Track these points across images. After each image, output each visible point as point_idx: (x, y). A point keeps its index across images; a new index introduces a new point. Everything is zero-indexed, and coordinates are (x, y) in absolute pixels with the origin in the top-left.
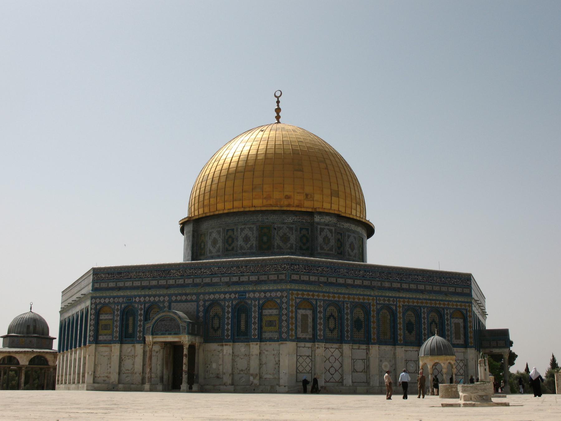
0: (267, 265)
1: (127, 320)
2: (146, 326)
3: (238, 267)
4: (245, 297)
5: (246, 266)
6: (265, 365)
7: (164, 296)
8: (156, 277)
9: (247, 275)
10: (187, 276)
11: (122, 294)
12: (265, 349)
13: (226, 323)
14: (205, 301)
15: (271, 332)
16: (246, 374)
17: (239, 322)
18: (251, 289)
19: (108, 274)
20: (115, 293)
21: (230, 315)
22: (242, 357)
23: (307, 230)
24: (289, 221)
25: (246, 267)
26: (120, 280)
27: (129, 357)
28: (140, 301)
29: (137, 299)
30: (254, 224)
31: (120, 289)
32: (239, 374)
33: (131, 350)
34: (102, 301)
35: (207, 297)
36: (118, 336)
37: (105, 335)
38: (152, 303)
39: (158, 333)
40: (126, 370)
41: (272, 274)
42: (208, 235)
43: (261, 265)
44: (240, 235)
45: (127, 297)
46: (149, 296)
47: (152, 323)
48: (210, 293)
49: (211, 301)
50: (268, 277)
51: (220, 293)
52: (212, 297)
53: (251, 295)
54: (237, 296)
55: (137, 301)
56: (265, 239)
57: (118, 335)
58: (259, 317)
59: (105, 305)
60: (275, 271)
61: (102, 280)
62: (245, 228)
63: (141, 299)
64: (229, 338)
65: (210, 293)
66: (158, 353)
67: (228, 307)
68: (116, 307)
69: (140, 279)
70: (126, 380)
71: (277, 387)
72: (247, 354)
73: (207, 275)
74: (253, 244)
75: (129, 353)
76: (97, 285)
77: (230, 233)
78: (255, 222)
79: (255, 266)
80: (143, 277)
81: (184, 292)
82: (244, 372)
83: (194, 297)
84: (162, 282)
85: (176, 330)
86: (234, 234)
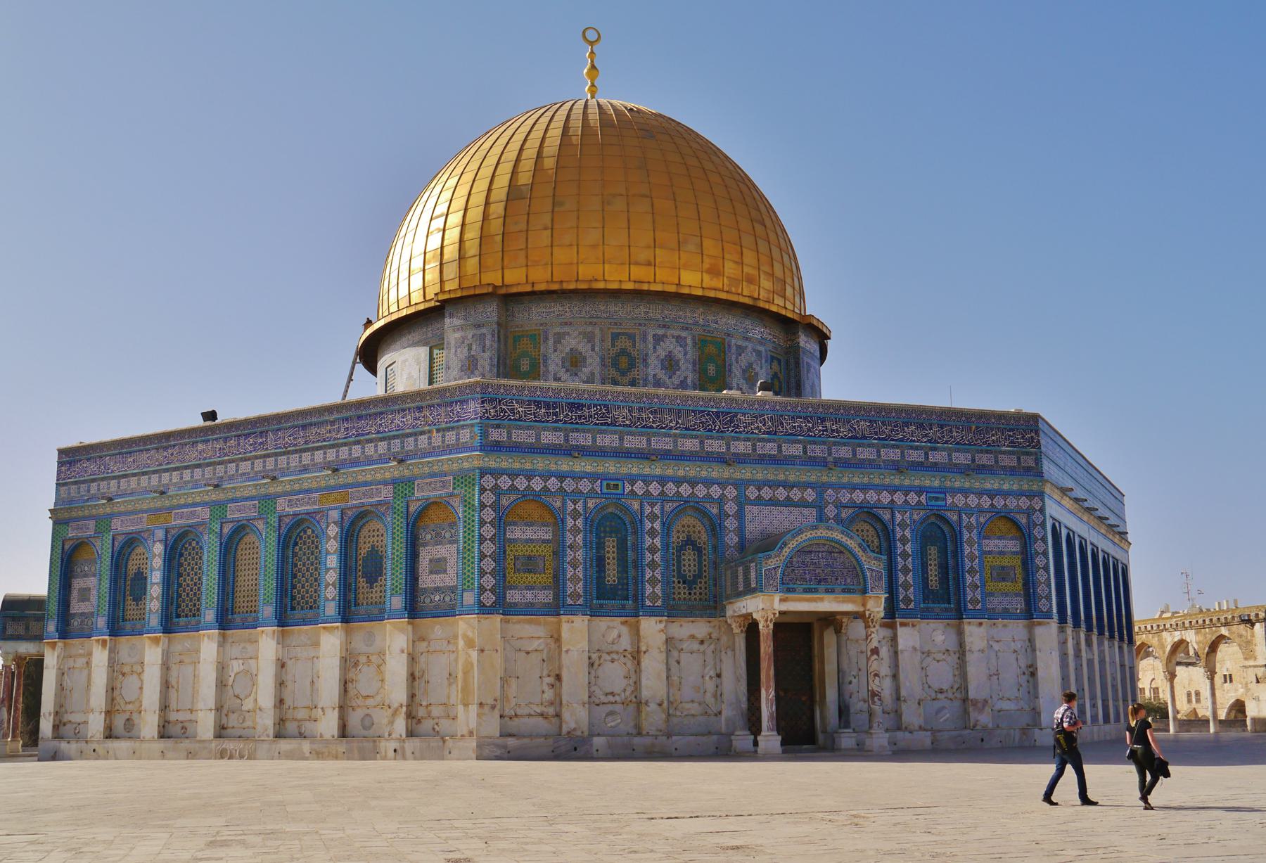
1: (600, 546)
2: (764, 564)
3: (921, 426)
4: (943, 503)
5: (942, 427)
6: (996, 677)
7: (722, 484)
8: (694, 430)
9: (944, 449)
10: (785, 435)
11: (589, 469)
12: (993, 638)
13: (900, 567)
14: (840, 506)
15: (1007, 594)
16: (951, 699)
17: (924, 566)
18: (957, 484)
19: (538, 404)
20: (565, 465)
21: (908, 548)
22: (940, 656)
23: (779, 361)
24: (755, 336)
26: (577, 426)
27: (615, 656)
28: (648, 493)
29: (639, 488)
30: (687, 329)
31: (584, 452)
32: (934, 699)
33: (620, 636)
34: (521, 483)
35: (845, 497)
36: (581, 591)
37: (528, 588)
38: (685, 502)
39: (795, 586)
40: (607, 694)
41: (1004, 453)
42: (546, 339)
43: (977, 428)
44: (655, 352)
45: (603, 477)
46: (678, 482)
47: (783, 558)
48: (853, 488)
50: (996, 457)
51: (880, 488)
52: (858, 497)
53: (959, 500)
54: (923, 499)
55: (640, 492)
56: (712, 369)
57: (580, 588)
59: (529, 496)
60: (1012, 447)
61: (515, 420)
62: (665, 336)
63: (651, 488)
64: (912, 606)
65: (853, 488)
66: (706, 645)
67: (903, 525)
68: (570, 506)
69: (643, 430)
70: (609, 725)
71: (1036, 731)
73: (842, 438)
75: (613, 643)
76: (495, 435)
77: (623, 343)
78: (691, 326)
81: (781, 477)
83: (810, 495)
84: (716, 446)
85: (849, 580)
86: (634, 346)
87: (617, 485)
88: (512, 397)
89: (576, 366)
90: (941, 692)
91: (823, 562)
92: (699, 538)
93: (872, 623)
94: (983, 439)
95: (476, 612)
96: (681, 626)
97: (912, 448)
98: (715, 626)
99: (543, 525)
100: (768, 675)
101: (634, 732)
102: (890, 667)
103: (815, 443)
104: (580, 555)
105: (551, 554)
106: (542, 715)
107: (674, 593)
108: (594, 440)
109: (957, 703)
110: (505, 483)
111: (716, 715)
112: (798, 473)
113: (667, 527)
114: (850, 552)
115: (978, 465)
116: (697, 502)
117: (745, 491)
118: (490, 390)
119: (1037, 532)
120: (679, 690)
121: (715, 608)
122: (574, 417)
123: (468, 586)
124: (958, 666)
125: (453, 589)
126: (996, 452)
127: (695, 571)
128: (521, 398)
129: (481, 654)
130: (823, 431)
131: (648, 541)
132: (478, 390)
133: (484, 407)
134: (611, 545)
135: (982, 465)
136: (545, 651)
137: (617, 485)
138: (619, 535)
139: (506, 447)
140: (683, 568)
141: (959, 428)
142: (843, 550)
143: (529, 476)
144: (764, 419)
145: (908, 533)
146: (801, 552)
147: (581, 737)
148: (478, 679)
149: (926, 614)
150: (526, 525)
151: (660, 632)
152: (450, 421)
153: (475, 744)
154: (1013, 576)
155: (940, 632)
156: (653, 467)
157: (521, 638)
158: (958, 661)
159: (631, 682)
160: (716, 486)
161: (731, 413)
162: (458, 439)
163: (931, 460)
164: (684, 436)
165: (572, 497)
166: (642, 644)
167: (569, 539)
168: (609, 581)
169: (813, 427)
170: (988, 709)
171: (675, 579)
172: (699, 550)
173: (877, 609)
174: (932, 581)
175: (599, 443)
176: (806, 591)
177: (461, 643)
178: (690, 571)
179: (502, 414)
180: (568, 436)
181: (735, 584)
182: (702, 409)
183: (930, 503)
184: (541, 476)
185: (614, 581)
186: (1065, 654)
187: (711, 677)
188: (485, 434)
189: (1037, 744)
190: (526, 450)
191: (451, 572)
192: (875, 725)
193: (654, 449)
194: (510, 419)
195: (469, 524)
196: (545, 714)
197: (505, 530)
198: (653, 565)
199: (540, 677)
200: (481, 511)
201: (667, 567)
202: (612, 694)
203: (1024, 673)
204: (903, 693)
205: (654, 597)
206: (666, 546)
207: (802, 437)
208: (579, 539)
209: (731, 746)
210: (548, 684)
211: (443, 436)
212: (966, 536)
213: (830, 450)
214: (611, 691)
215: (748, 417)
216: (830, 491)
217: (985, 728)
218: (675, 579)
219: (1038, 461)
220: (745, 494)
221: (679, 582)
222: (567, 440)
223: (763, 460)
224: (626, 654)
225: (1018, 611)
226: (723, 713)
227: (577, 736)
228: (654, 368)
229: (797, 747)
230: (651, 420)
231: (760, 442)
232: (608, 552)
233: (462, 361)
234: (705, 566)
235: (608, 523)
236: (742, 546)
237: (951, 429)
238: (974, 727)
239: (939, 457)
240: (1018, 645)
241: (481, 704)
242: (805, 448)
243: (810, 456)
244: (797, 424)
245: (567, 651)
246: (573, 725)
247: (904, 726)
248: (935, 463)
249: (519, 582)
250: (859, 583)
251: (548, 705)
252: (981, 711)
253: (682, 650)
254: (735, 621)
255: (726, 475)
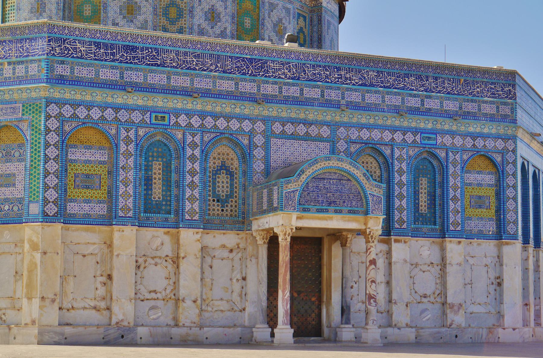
0: (477, 83)
1: (148, 168)
3: (419, 78)
5: (436, 79)
6: (471, 285)
7: (253, 120)
8: (230, 73)
9: (437, 98)
10: (306, 80)
11: (140, 102)
15: (482, 219)
16: (433, 303)
17: (416, 193)
18: (446, 127)
19: (98, 45)
21: (404, 178)
22: (426, 268)
23: (305, 18)
25: (437, 80)
26: (131, 65)
27: (157, 260)
28: (190, 125)
32: (419, 303)
35: (354, 134)
36: (131, 206)
37: (87, 201)
38: (221, 133)
39: (310, 207)
40: (150, 292)
41: (486, 102)
43: (465, 81)
45: (153, 110)
46: (216, 116)
47: (300, 183)
49: (363, 143)
50: (479, 106)
51: (383, 128)
52: (365, 134)
53: (447, 140)
56: (248, 22)
57: (130, 203)
58: (461, 188)
60: (493, 97)
63: (193, 121)
64: (404, 226)
65: (361, 127)
66: (234, 253)
67: (400, 159)
68: (123, 134)
69: (188, 71)
70: (151, 317)
71: (500, 330)
72: (432, 262)
74: (225, 29)
75: (157, 250)
76: (60, 70)
79: (453, 81)
80: (197, 68)
81: (302, 116)
82: (428, 299)
83: (325, 132)
84: (248, 87)
85: (354, 203)
87: (164, 117)
88: (75, 37)
89: (132, 14)
90: (425, 297)
91: (333, 187)
92: (232, 164)
93: (372, 238)
94: (469, 90)
95: (41, 220)
96: (214, 237)
97: (411, 95)
98: (242, 238)
99: (100, 148)
100: (285, 279)
101: (172, 323)
102: (384, 275)
103: (331, 88)
104: (131, 175)
105: (107, 173)
106: (95, 308)
107: (209, 210)
108: (145, 78)
109: (438, 306)
110: (67, 111)
111: (241, 311)
112: (316, 113)
113: (205, 154)
114: (356, 180)
115: (465, 112)
116: (231, 134)
117: (271, 126)
118: (56, 30)
119: (509, 169)
120: (211, 290)
121: (243, 223)
122: (128, 58)
123: (34, 199)
124: (440, 276)
125: (20, 201)
126: (479, 101)
127: (227, 192)
128: (83, 39)
129: (44, 256)
130: (338, 78)
131: (189, 166)
132: (45, 29)
133: (50, 45)
134: (157, 167)
135: (467, 112)
136: (99, 255)
137: (164, 117)
138: (164, 160)
139: (70, 81)
140: (217, 189)
141: (450, 81)
142: (349, 178)
143: (89, 106)
144: (290, 66)
145: (404, 166)
146: (317, 178)
147: (128, 326)
148: (41, 277)
149: (416, 233)
150: (85, 147)
151: (197, 241)
152: (20, 56)
153: (36, 331)
154: (488, 204)
155: (426, 248)
156: (195, 103)
157: (79, 243)
158: (440, 272)
159: (171, 283)
160: (247, 121)
161: (262, 60)
162: (27, 72)
163: (427, 106)
164: (221, 78)
165: (126, 126)
166: (182, 251)
167: (122, 161)
168: (154, 198)
169: (330, 75)
170: (462, 312)
171: (210, 198)
172: (231, 174)
173: (376, 228)
174: (422, 206)
175: (150, 80)
176: (319, 211)
177: (27, 246)
178: (223, 191)
179: (66, 52)
180: (123, 73)
181: (260, 203)
182: (238, 55)
183: (423, 142)
184: (99, 107)
185: (159, 198)
186: (526, 269)
187: (238, 280)
188: (50, 69)
189: (500, 340)
190: (87, 84)
191: (19, 186)
192: (370, 322)
193: (196, 88)
194: (73, 57)
195: (36, 145)
196: (98, 307)
197: (67, 152)
198: (192, 185)
199: (95, 277)
200: (46, 134)
201: (204, 187)
202: (155, 292)
203: (492, 284)
204: (395, 296)
205: (192, 212)
206: (204, 170)
207: (321, 83)
208: (131, 162)
209: (253, 336)
210: (101, 282)
211: (14, 69)
212: (451, 170)
213: (343, 94)
214: (154, 289)
215: (276, 64)
216: (342, 129)
217: (459, 327)
218: (210, 198)
219: (513, 110)
220: (271, 129)
221: (214, 201)
222: (122, 77)
223: (287, 101)
224: (168, 259)
225: (491, 233)
226: (247, 309)
227: (124, 326)
228: (199, 19)
229: (306, 339)
230: (194, 63)
231: (286, 85)
232: (155, 174)
233: (32, 4)
234: (236, 188)
235: (155, 149)
236: (267, 173)
237: (444, 81)
238: (450, 326)
239: (431, 104)
240: (489, 261)
241: (43, 298)
242: (323, 92)
243: (327, 100)
244: (316, 72)
245: (118, 255)
246: (121, 317)
247: (393, 324)
248: (429, 109)
249: (78, 196)
250: (362, 206)
251: (101, 300)
252: (456, 313)
253: (214, 257)
254: (259, 234)
255: (256, 112)
